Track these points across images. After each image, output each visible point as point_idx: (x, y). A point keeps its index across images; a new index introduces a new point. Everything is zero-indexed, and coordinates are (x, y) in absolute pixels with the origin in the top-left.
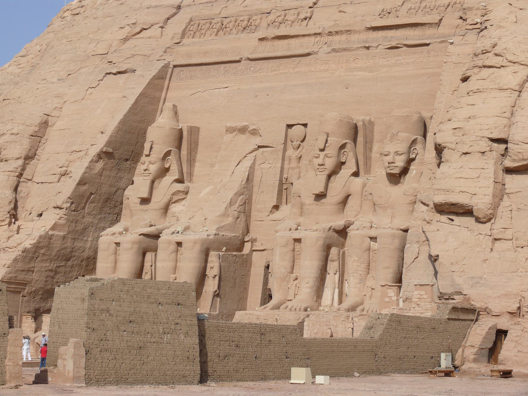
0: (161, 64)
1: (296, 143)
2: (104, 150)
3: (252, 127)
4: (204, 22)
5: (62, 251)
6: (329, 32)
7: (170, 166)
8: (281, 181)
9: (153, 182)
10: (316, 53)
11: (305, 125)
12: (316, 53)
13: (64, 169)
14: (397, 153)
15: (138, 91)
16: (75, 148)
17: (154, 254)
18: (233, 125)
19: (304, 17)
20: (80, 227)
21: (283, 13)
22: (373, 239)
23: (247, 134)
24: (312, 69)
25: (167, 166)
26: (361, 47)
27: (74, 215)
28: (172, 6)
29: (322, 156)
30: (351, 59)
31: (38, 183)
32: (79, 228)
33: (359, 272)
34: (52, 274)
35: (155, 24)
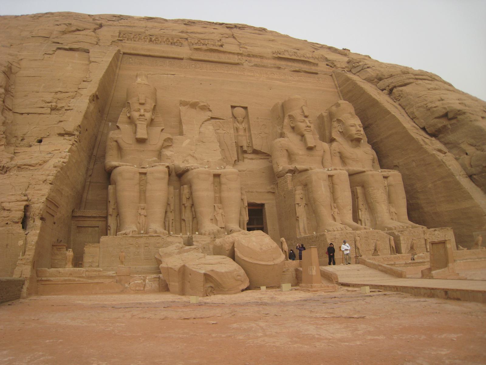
1: (240, 119)
2: (97, 93)
3: (202, 104)
6: (248, 54)
10: (242, 65)
11: (245, 108)
12: (242, 65)
13: (54, 104)
18: (187, 99)
19: (220, 44)
22: (385, 177)
23: (198, 109)
24: (242, 74)
25: (153, 117)
26: (274, 67)
31: (22, 114)
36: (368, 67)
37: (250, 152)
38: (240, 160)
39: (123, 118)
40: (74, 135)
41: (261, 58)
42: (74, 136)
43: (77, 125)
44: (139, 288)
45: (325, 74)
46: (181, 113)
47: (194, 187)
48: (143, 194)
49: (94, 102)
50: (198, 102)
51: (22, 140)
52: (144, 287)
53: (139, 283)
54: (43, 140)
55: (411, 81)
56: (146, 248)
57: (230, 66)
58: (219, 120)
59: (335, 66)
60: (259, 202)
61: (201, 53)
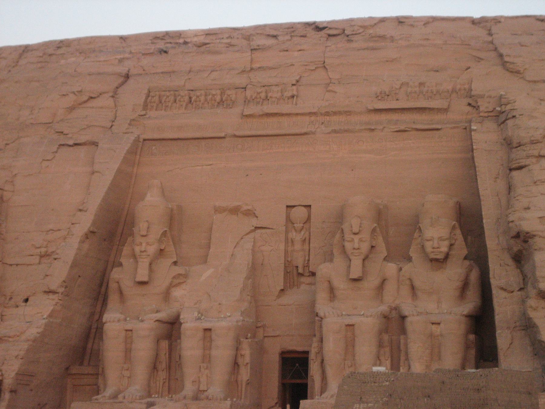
0: (132, 138)
1: (298, 225)
2: (91, 229)
3: (245, 208)
4: (168, 94)
8: (285, 264)
9: (150, 264)
10: (314, 133)
12: (314, 133)
13: (43, 250)
14: (441, 239)
15: (116, 166)
16: (51, 227)
17: (167, 342)
19: (290, 94)
21: (263, 89)
25: (163, 247)
26: (365, 129)
28: (119, 75)
29: (356, 241)
31: (11, 265)
33: (425, 358)
35: (104, 93)
36: (514, 117)
39: (126, 250)
41: (348, 114)
42: (57, 295)
45: (454, 128)
46: (214, 226)
48: (128, 352)
49: (88, 240)
51: (11, 298)
55: (527, 162)
59: (478, 107)
60: (300, 349)
61: (254, 120)
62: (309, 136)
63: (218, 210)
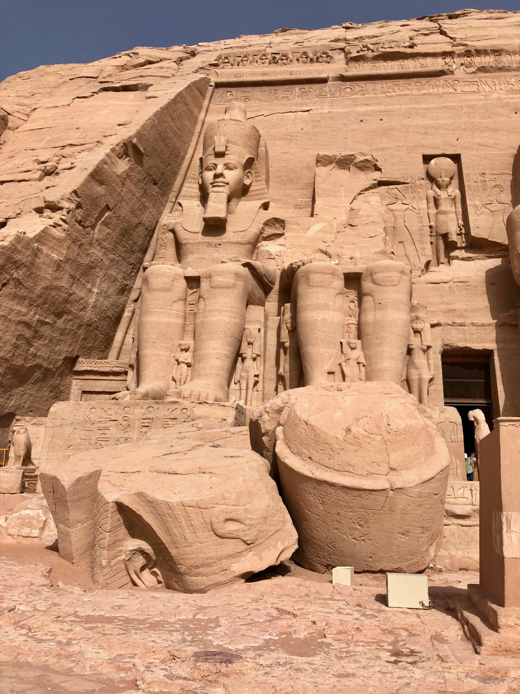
2: (135, 141)
3: (361, 158)
5: (53, 293)
7: (251, 183)
9: (229, 201)
10: (452, 73)
11: (456, 158)
12: (452, 73)
20: (85, 260)
23: (352, 168)
24: (451, 90)
25: (247, 182)
27: (78, 231)
30: (513, 80)
32: (82, 261)
34: (28, 334)
37: (464, 245)
38: (443, 263)
40: (61, 209)
43: (71, 191)
44: (29, 530)
46: (317, 178)
47: (301, 303)
49: (128, 159)
50: (353, 155)
52: (43, 529)
53: (31, 518)
54: (8, 223)
56: (144, 429)
57: (423, 81)
58: (397, 186)
61: (366, 64)
62: (446, 77)
63: (322, 161)
